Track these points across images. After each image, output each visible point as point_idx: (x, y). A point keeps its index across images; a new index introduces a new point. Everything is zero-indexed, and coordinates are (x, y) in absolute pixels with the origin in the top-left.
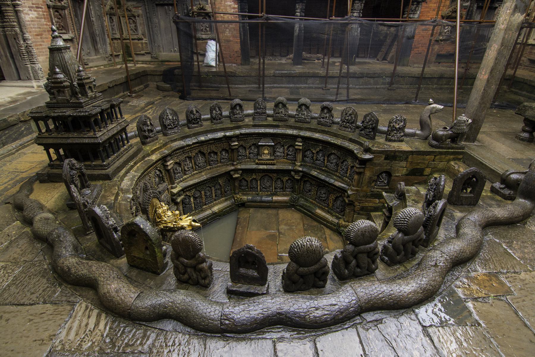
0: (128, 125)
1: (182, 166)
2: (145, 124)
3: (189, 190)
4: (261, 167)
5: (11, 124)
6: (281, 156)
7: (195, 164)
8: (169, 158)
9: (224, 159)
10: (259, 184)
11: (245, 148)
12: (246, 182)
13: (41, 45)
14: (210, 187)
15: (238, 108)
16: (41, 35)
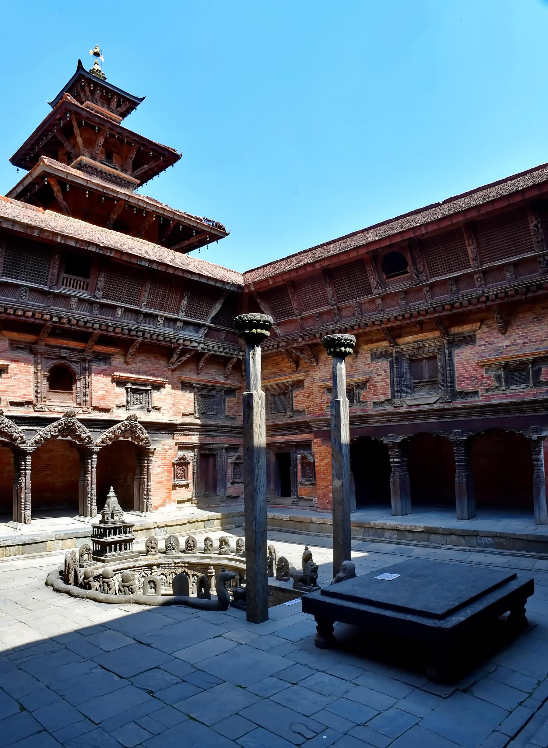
0: (134, 539)
15: (224, 543)
16: (162, 482)
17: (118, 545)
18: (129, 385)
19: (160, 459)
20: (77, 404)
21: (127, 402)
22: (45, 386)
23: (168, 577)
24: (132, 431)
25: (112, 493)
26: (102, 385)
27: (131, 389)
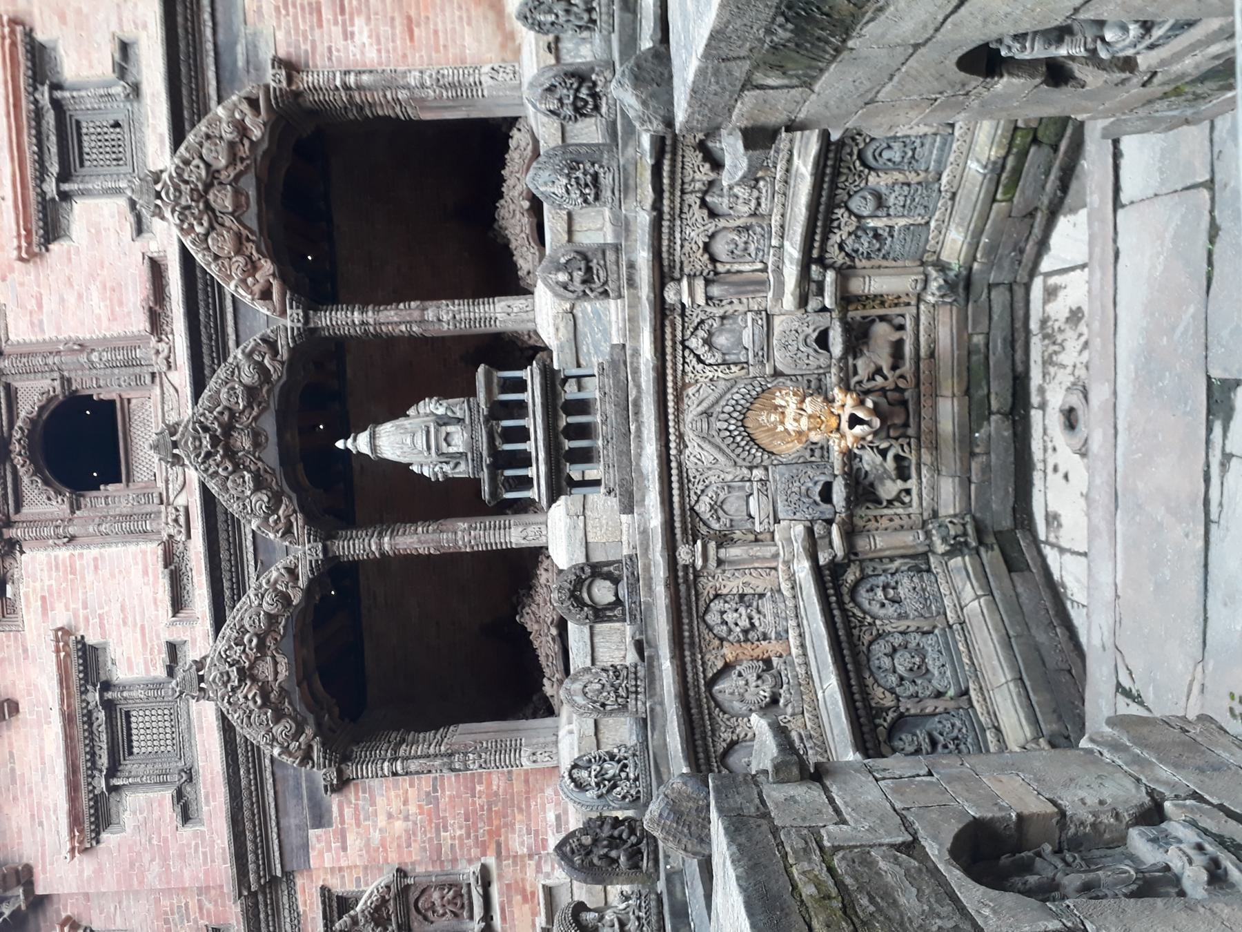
5: (572, 336)
8: (670, 296)
13: (436, 32)
16: (409, 19)
17: (568, 444)
18: (50, 187)
19: (317, 32)
20: (153, 381)
21: (118, 191)
22: (113, 498)
24: (208, 186)
25: (361, 444)
26: (71, 299)
27: (64, 176)
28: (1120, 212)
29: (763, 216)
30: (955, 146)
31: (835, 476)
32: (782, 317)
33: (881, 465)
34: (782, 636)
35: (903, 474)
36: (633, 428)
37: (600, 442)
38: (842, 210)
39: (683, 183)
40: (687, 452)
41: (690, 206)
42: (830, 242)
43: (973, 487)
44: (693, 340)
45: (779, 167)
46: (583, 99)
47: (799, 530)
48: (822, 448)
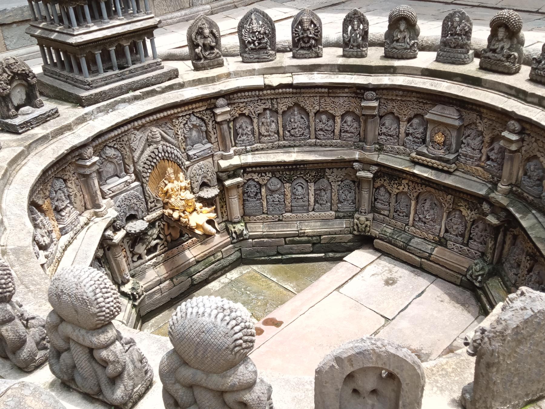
1: (255, 125)
2: (200, 32)
3: (259, 173)
4: (417, 171)
6: (472, 158)
7: (284, 127)
8: (221, 101)
9: (346, 132)
10: (412, 208)
11: (398, 119)
12: (387, 195)
14: (307, 181)
15: (402, 27)
17: (112, 49)
23: (255, 121)
28: (336, 292)
29: (259, 139)
30: (305, 214)
31: (143, 219)
32: (212, 162)
33: (153, 239)
34: (63, 231)
35: (149, 252)
36: (137, 93)
37: (117, 71)
38: (271, 176)
39: (277, 99)
40: (136, 132)
41: (265, 103)
42: (253, 174)
43: (158, 287)
44: (195, 118)
45: (284, 142)
46: (308, 42)
47: (116, 214)
48: (156, 206)
